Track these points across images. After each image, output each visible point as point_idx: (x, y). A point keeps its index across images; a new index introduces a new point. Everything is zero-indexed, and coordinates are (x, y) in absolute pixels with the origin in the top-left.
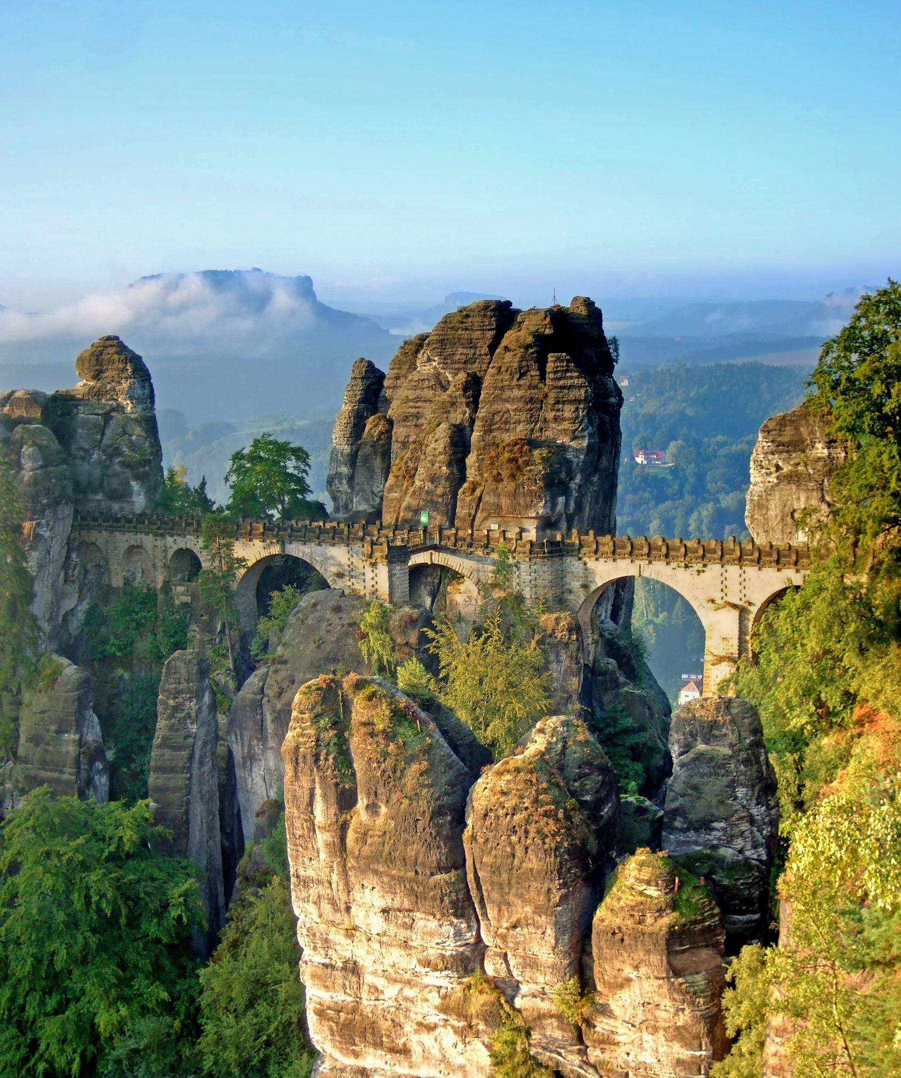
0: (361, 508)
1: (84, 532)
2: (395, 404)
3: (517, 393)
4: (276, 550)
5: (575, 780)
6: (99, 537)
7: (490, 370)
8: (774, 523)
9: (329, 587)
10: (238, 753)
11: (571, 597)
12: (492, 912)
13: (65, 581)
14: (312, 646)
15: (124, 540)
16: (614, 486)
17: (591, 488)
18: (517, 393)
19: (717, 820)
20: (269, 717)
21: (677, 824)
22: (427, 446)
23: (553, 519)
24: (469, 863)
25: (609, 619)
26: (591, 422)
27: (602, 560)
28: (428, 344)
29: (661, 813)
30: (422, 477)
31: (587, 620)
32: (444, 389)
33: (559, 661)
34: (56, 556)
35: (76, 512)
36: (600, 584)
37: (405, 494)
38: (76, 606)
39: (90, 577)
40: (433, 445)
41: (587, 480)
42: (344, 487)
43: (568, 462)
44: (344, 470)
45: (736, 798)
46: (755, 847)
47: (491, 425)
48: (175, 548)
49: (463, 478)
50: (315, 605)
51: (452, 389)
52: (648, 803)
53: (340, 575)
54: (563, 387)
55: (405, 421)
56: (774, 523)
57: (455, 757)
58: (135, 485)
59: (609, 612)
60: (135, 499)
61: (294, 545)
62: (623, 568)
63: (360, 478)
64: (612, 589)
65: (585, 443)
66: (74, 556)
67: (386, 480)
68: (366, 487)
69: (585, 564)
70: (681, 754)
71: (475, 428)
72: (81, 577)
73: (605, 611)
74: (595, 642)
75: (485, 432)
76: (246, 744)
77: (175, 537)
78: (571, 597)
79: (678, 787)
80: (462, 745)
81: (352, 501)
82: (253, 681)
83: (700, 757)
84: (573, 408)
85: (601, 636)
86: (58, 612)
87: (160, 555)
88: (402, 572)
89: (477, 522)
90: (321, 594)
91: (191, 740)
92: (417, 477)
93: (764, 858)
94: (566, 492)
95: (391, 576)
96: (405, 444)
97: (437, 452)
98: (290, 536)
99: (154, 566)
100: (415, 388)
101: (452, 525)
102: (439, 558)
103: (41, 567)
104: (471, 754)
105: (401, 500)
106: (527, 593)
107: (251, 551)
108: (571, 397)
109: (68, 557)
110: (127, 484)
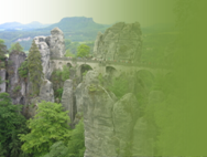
82: (79, 85)
107: (80, 64)
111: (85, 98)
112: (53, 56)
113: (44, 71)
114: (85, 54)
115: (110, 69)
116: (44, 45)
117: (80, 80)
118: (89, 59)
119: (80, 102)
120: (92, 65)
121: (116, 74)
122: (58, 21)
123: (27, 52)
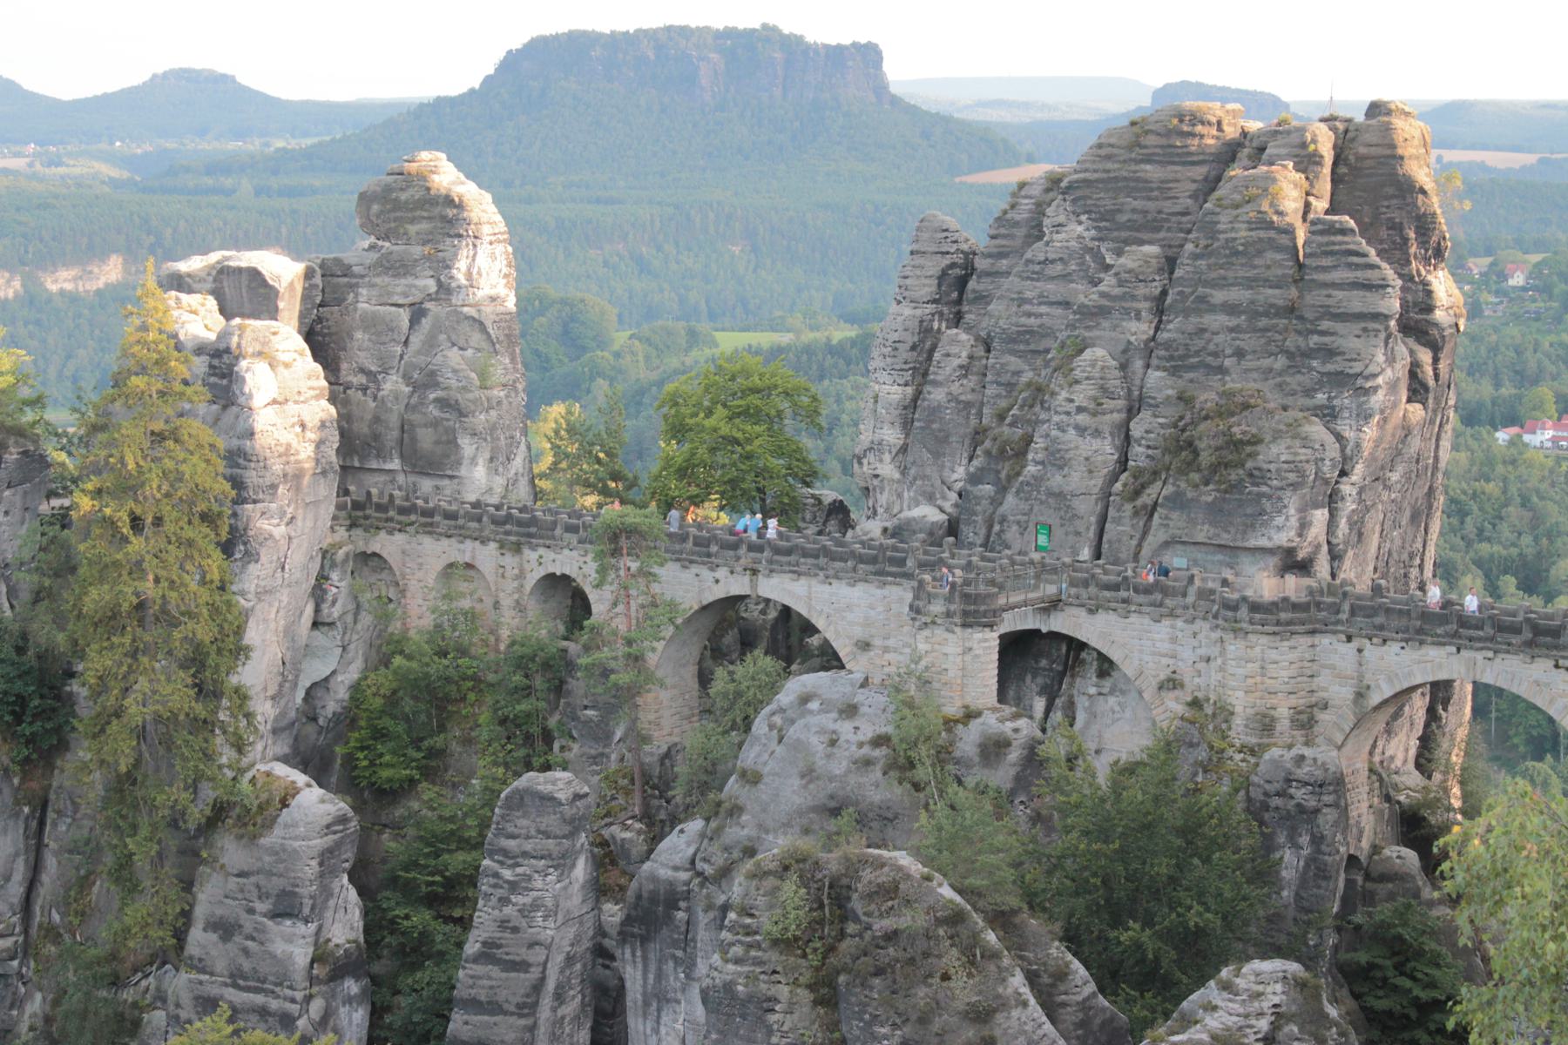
0: (917, 512)
1: (358, 532)
4: (736, 585)
6: (388, 544)
7: (1189, 247)
9: (842, 667)
11: (1323, 717)
13: (316, 624)
14: (796, 782)
17: (1385, 496)
22: (1053, 394)
23: (1301, 555)
25: (1411, 766)
26: (1391, 360)
27: (1394, 647)
28: (1069, 188)
30: (1040, 456)
31: (1362, 765)
32: (1095, 283)
34: (298, 575)
36: (1388, 693)
37: (1003, 490)
38: (334, 672)
39: (366, 619)
40: (1064, 394)
42: (888, 469)
43: (1339, 437)
44: (892, 436)
47: (1187, 356)
48: (540, 572)
50: (805, 699)
53: (865, 646)
54: (1334, 285)
55: (1014, 341)
57: (1048, 1027)
58: (467, 445)
59: (1413, 752)
60: (463, 471)
61: (776, 580)
64: (1418, 706)
66: (335, 576)
67: (971, 459)
68: (928, 471)
69: (1360, 651)
71: (1154, 362)
72: (349, 618)
74: (1379, 814)
75: (1174, 371)
76: (653, 967)
77: (542, 551)
78: (1323, 717)
80: (1064, 1005)
81: (900, 496)
82: (679, 845)
84: (1356, 327)
85: (1388, 798)
86: (295, 685)
87: (511, 585)
88: (986, 644)
89: (1146, 551)
91: (538, 955)
92: (1030, 456)
94: (1333, 500)
96: (1010, 386)
97: (1071, 407)
98: (770, 562)
99: (496, 605)
100: (1038, 276)
101: (1098, 555)
102: (1058, 623)
104: (1082, 1024)
105: (996, 501)
109: (322, 577)
110: (453, 443)
113: (256, 673)
114: (745, 457)
117: (658, 796)
121: (1116, 732)
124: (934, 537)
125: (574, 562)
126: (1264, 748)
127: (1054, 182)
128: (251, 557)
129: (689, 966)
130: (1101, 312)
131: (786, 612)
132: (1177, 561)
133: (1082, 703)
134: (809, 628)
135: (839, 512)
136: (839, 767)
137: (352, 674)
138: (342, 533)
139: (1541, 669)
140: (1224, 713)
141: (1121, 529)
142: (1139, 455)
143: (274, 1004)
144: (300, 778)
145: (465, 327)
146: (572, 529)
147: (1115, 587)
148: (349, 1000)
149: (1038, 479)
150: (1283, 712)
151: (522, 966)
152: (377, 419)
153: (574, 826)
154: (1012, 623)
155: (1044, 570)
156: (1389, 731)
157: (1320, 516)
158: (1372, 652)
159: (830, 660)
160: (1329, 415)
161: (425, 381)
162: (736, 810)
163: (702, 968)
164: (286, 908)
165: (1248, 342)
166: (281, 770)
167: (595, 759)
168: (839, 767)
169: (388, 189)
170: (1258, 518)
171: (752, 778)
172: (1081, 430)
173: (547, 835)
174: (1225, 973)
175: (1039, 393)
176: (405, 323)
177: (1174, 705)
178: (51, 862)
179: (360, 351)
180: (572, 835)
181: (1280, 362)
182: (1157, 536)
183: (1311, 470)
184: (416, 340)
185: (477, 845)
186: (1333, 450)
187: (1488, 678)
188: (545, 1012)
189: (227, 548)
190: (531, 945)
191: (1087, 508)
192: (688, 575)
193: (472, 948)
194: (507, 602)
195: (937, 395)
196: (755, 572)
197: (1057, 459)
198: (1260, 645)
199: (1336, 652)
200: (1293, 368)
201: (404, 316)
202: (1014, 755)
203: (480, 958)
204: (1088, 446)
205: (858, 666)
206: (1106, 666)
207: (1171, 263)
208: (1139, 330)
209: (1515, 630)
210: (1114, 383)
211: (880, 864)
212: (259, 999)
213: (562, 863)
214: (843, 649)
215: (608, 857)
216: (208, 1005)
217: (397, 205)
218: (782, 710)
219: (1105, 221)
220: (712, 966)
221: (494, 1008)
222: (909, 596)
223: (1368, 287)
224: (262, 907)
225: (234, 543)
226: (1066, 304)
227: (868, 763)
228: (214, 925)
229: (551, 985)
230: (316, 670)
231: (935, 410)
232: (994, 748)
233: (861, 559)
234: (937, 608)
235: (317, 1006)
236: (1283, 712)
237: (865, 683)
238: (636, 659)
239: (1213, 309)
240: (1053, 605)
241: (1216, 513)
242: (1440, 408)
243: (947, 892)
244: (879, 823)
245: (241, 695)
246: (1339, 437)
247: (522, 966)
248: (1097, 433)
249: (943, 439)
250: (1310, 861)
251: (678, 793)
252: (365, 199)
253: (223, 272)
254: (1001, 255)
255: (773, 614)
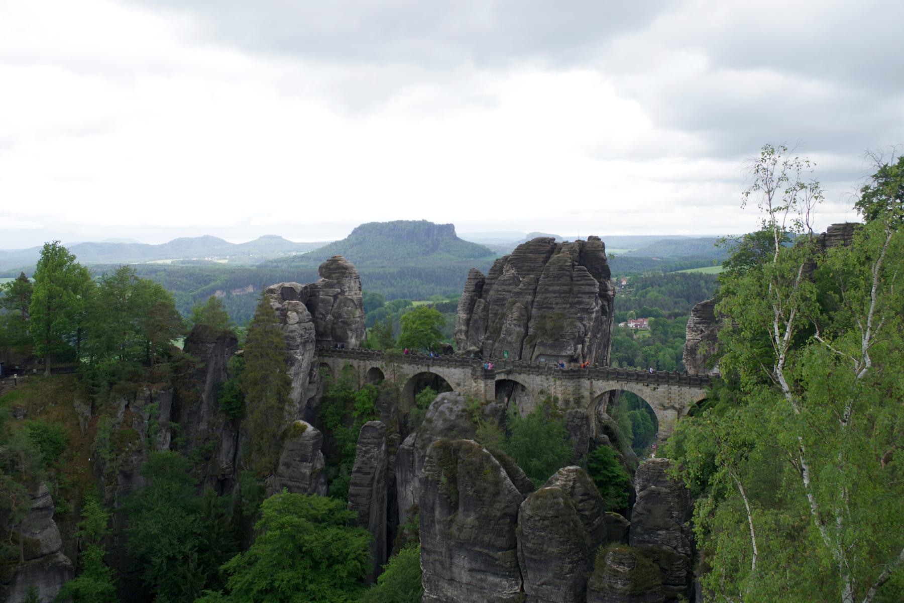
2: (491, 293)
3: (557, 288)
4: (424, 369)
5: (580, 502)
8: (699, 362)
10: (399, 479)
11: (583, 400)
12: (530, 575)
13: (310, 383)
14: (441, 422)
15: (341, 362)
16: (608, 340)
18: (557, 288)
19: (661, 529)
20: (417, 460)
21: (639, 530)
24: (519, 546)
26: (597, 304)
29: (629, 523)
31: (593, 413)
33: (576, 435)
35: (317, 346)
36: (599, 393)
37: (494, 341)
41: (594, 336)
42: (463, 337)
43: (584, 325)
44: (463, 328)
45: (672, 517)
46: (684, 546)
49: (526, 334)
50: (444, 399)
51: (521, 285)
52: (622, 517)
53: (459, 385)
56: (699, 362)
57: (513, 487)
62: (613, 385)
63: (472, 332)
65: (594, 315)
70: (641, 490)
73: (602, 408)
75: (539, 309)
78: (583, 400)
79: (639, 509)
82: (409, 440)
83: (652, 491)
88: (492, 384)
89: (534, 357)
90: (447, 394)
93: (689, 553)
94: (583, 342)
95: (486, 385)
100: (503, 284)
101: (520, 358)
102: (511, 377)
103: (297, 374)
105: (493, 345)
106: (559, 396)
107: (410, 370)
108: (587, 290)
109: (312, 370)
111: (425, 482)
112: (328, 339)
113: (296, 393)
115: (506, 388)
116: (297, 316)
118: (445, 354)
119: (410, 493)
120: (451, 374)
121: (526, 407)
122: (342, 235)
123: (241, 330)
124: (476, 353)
125: (377, 364)
126: (567, 409)
127: (506, 259)
128: (292, 364)
129: (413, 472)
130: (521, 293)
131: (437, 376)
132: (543, 360)
133: (518, 399)
134: (444, 380)
135: (449, 349)
136: (453, 418)
137: (320, 396)
138: (317, 358)
139: (640, 386)
140: (556, 399)
141: (526, 352)
142: (531, 331)
143: (302, 485)
144: (306, 423)
145: (348, 302)
146: (378, 355)
147: (526, 367)
148: (322, 484)
149: (504, 338)
150: (571, 399)
151: (369, 473)
152: (325, 327)
153: (381, 435)
154: (498, 377)
155: (506, 363)
156: (599, 404)
157: (580, 346)
158: (594, 382)
159: (449, 389)
160: (581, 319)
161: (337, 316)
162: (426, 430)
163: (417, 473)
164: (304, 459)
165: (559, 300)
166: (302, 422)
167: (387, 417)
168: (453, 418)
169: (327, 265)
170: (563, 347)
171: (430, 421)
172: (515, 325)
173: (374, 438)
174: (561, 470)
175: (504, 316)
176: (332, 300)
177: (543, 398)
178: (240, 449)
179: (321, 308)
180: (381, 438)
181: (568, 306)
182: (537, 353)
183: (577, 335)
184: (335, 305)
185: (355, 441)
186: (583, 329)
187: (626, 389)
188: (375, 486)
189: (286, 361)
190: (371, 468)
191: (517, 345)
192: (410, 367)
193: (354, 469)
194: (361, 375)
195: (475, 317)
196: (428, 366)
197: (509, 333)
198: (566, 382)
199: (586, 383)
200: (571, 307)
201: (332, 299)
202: (500, 413)
203: (356, 472)
204: (517, 329)
205: (457, 390)
206: (523, 388)
207: (538, 280)
208: (530, 298)
209: (632, 375)
210: (524, 312)
211: (468, 443)
212: (297, 484)
213: (379, 445)
214: (453, 386)
215: (391, 443)
216: (283, 485)
217: (330, 269)
218: (437, 403)
219: (519, 268)
220: (422, 473)
221: (362, 486)
222: (470, 371)
223: (591, 285)
224: (298, 459)
225: (290, 361)
226: (510, 292)
227: (462, 416)
228: (285, 464)
229: (376, 478)
230: (312, 394)
231: (476, 321)
232: (495, 412)
233: (457, 361)
234: (479, 374)
235: (313, 485)
236: (571, 399)
237: (459, 395)
238: (398, 390)
239: (550, 292)
240: (509, 372)
241: (553, 347)
242: (610, 317)
243: (485, 450)
244: (465, 432)
245: (291, 403)
246: (584, 325)
247: (369, 473)
248: (519, 326)
249: (477, 329)
250: (580, 439)
251: (409, 425)
252: (321, 268)
253: (284, 289)
254: (493, 279)
255: (433, 377)
